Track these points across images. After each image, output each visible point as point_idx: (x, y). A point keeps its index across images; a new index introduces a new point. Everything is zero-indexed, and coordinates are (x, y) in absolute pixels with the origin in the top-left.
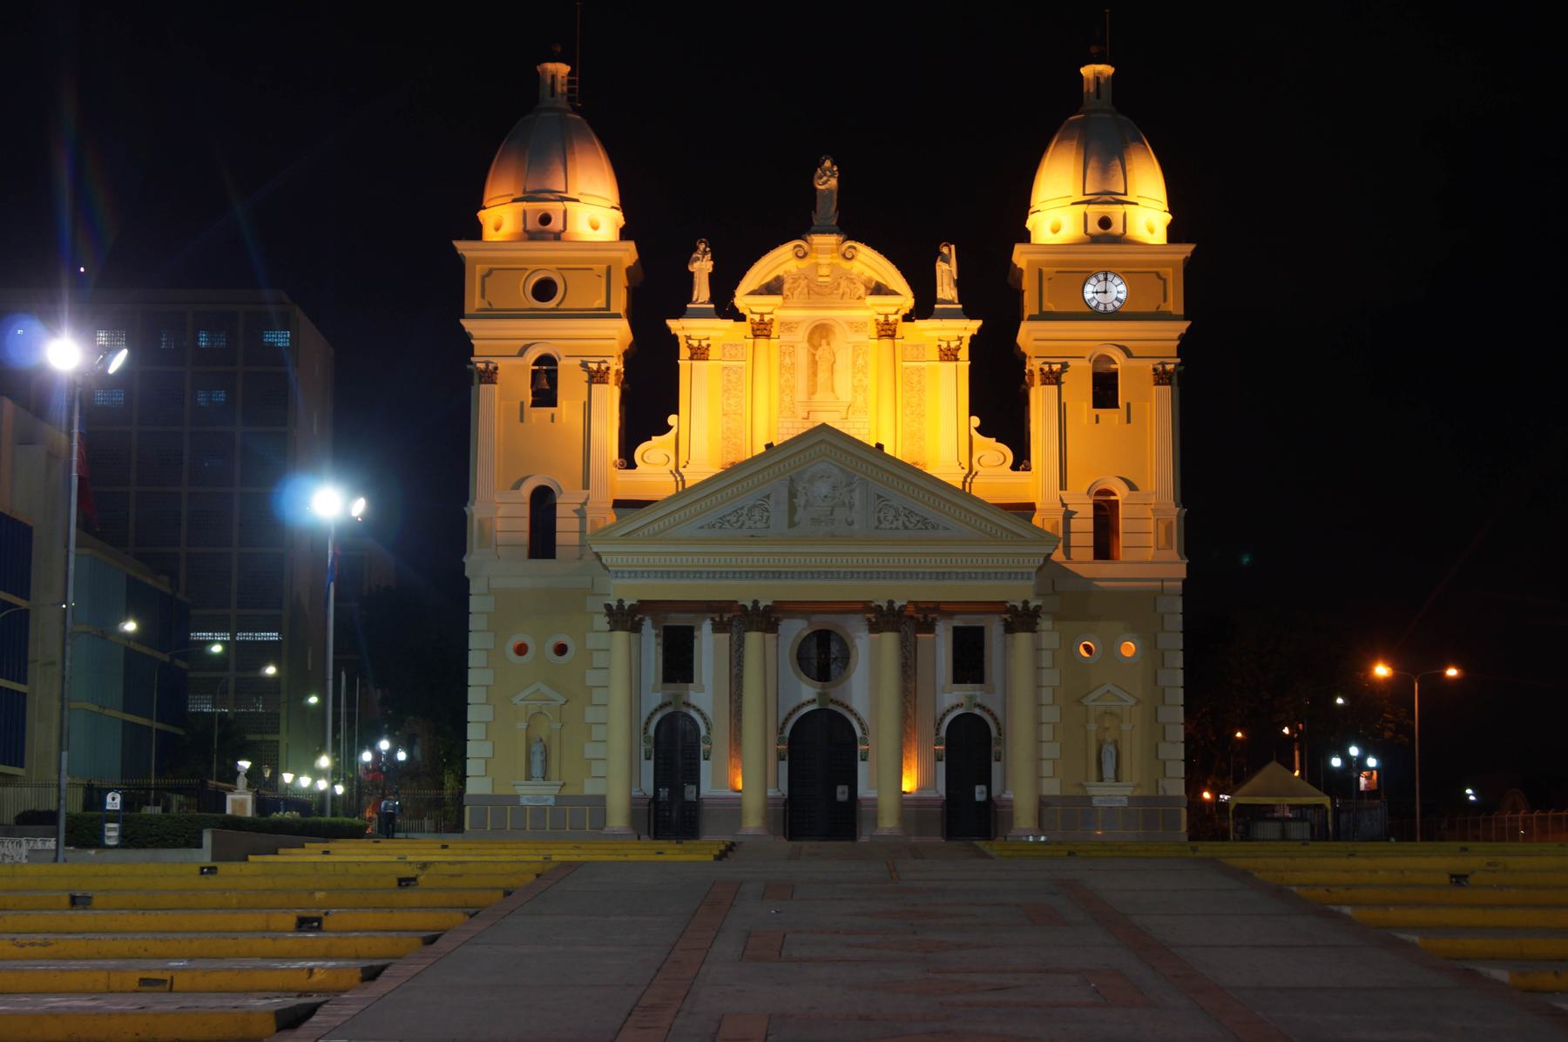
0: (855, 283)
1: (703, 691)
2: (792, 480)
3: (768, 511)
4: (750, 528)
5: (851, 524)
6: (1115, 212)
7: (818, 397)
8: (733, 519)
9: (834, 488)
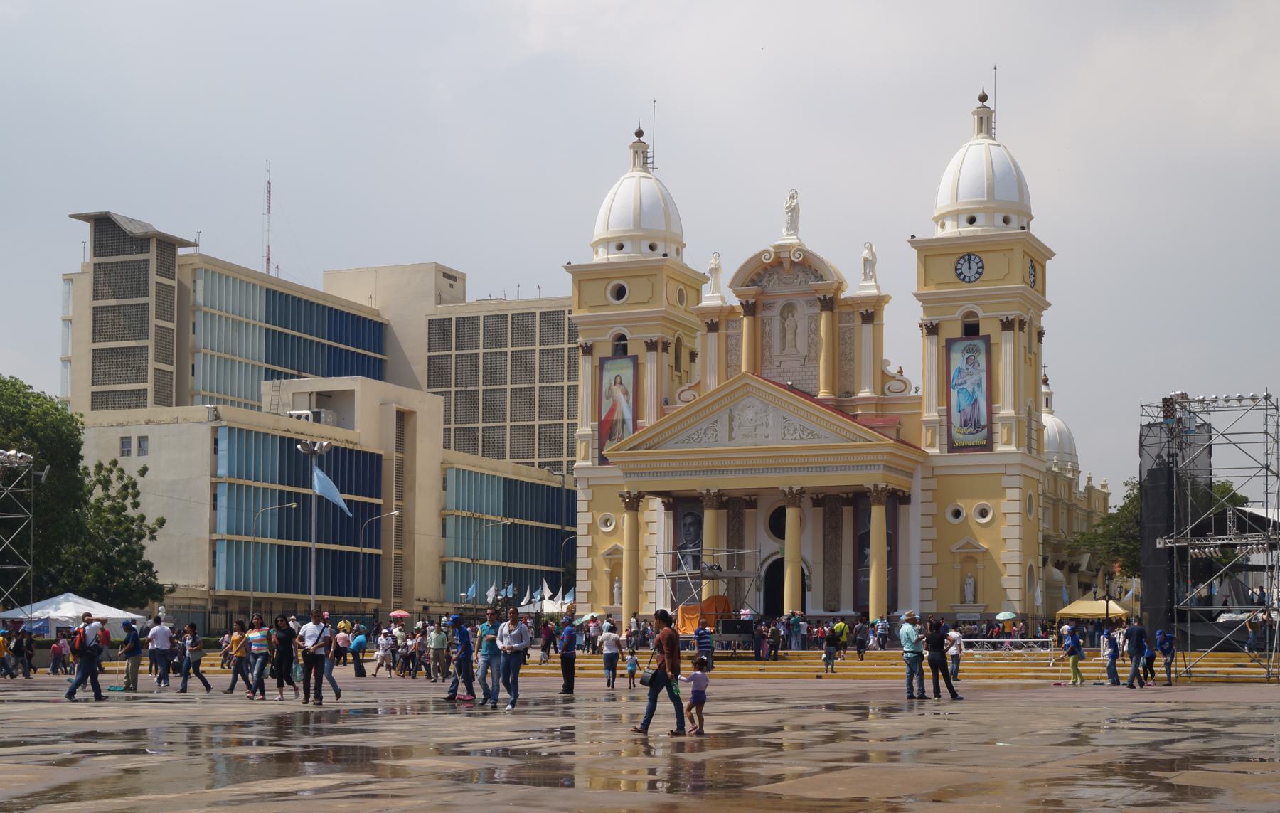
0: (807, 274)
2: (731, 410)
7: (785, 352)
8: (695, 437)
9: (757, 414)
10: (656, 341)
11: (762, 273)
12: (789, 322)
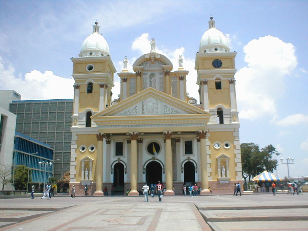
0: (159, 64)
1: (125, 157)
2: (143, 102)
3: (137, 110)
4: (132, 114)
5: (158, 112)
9: (153, 104)
10: (104, 84)
11: (143, 62)
12: (153, 80)
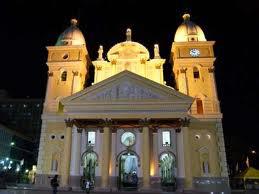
6: (195, 37)
